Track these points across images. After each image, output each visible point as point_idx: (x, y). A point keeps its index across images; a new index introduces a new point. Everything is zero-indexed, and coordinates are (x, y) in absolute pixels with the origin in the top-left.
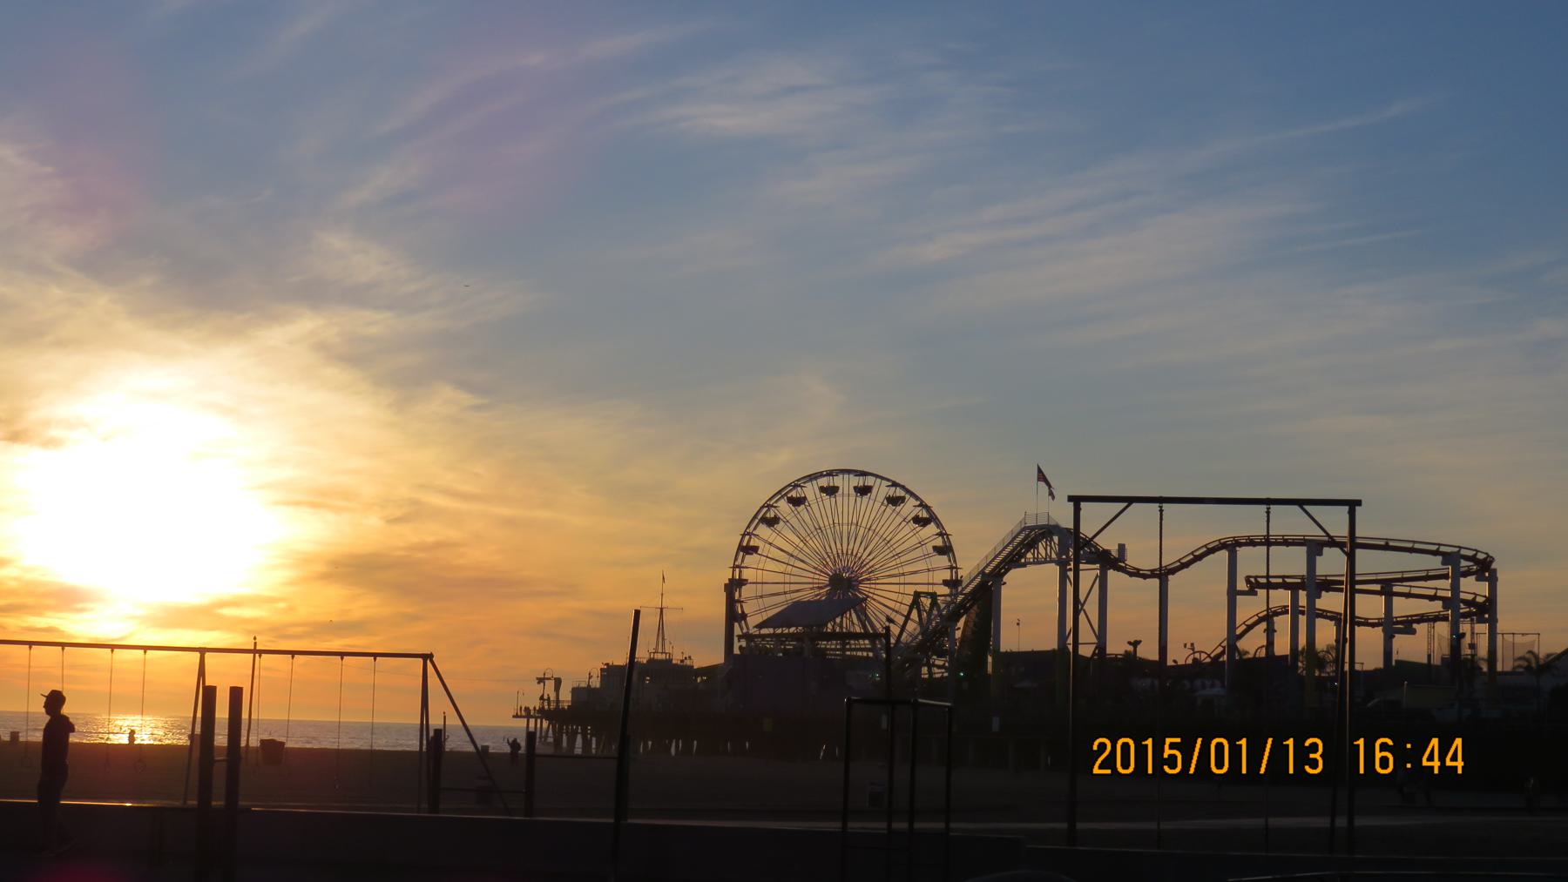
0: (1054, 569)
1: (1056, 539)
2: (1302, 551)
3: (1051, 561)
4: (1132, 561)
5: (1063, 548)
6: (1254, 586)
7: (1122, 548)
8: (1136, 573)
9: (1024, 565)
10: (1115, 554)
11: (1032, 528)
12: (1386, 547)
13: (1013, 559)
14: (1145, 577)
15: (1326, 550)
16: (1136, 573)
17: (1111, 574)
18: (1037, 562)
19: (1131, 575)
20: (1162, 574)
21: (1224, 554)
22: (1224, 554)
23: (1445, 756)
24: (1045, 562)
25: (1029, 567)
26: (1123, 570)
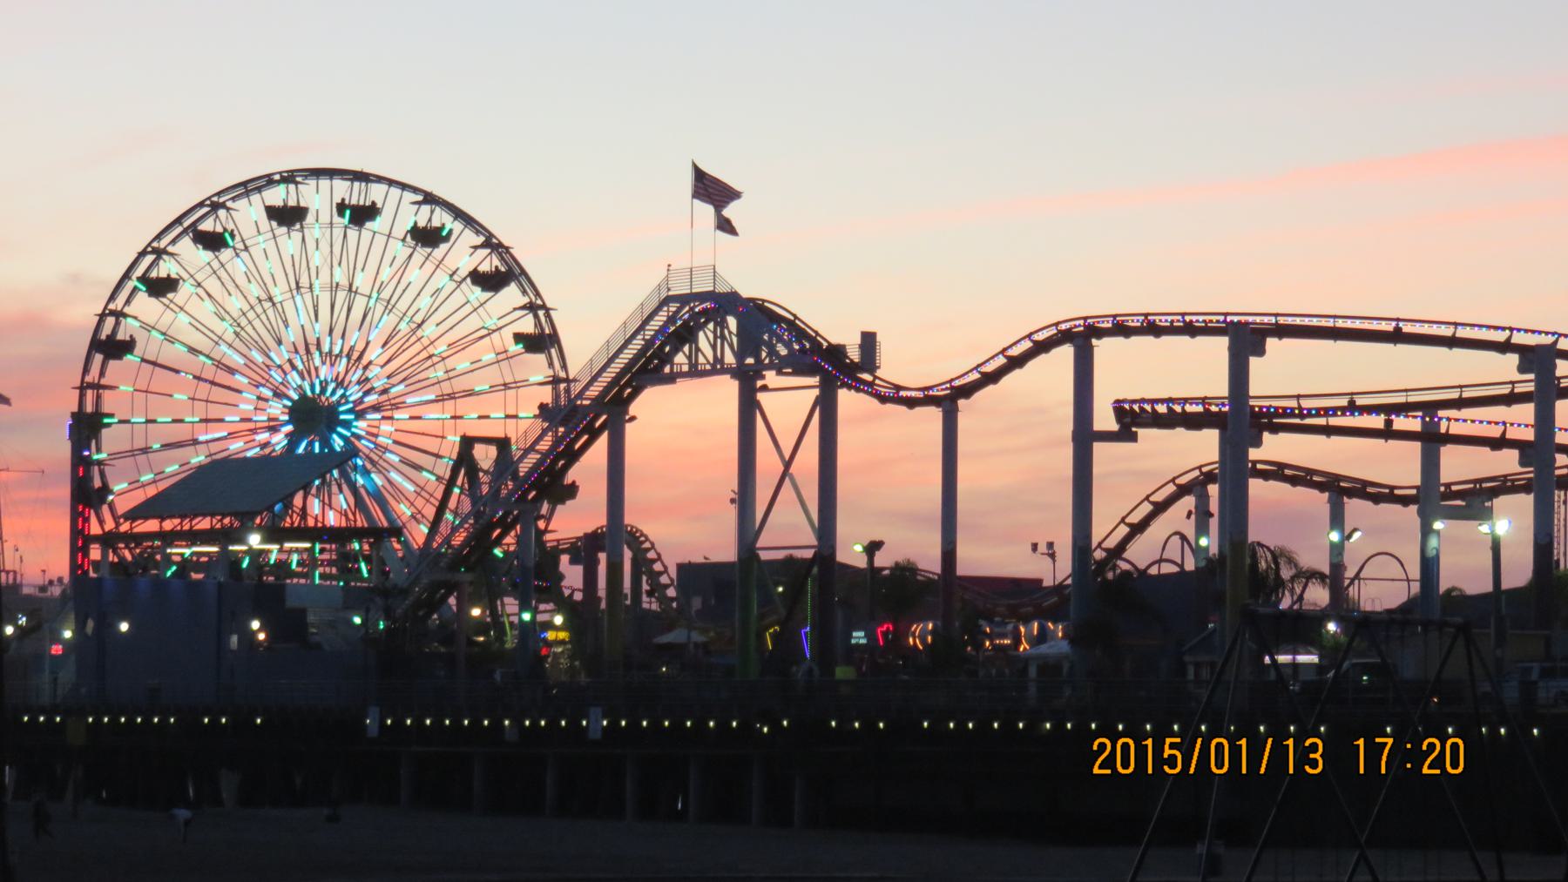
0: (728, 388)
1: (732, 322)
2: (1223, 342)
3: (723, 371)
4: (893, 368)
5: (748, 343)
6: (1132, 419)
7: (869, 341)
8: (895, 396)
9: (671, 379)
10: (854, 354)
11: (684, 299)
12: (1397, 337)
13: (650, 362)
14: (911, 403)
15: (1271, 342)
16: (895, 396)
17: (845, 397)
18: (695, 372)
19: (883, 399)
20: (949, 400)
21: (1066, 353)
22: (1066, 353)
23: (1446, 754)
24: (714, 371)
25: (682, 384)
26: (870, 389)
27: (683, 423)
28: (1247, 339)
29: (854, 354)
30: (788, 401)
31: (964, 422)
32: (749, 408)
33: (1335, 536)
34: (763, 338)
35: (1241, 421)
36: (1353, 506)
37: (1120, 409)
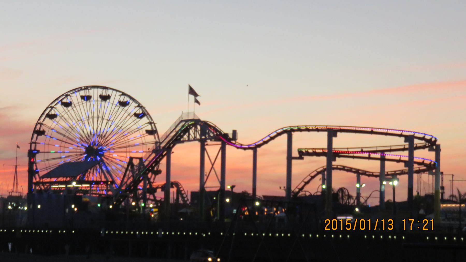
1: (199, 127)
4: (240, 140)
5: (203, 133)
6: (302, 154)
7: (235, 132)
9: (183, 142)
10: (231, 136)
11: (187, 121)
12: (372, 132)
14: (245, 149)
15: (339, 134)
16: (241, 147)
17: (228, 147)
18: (189, 140)
19: (238, 148)
20: (255, 148)
21: (285, 136)
22: (285, 136)
26: (234, 145)
28: (332, 133)
29: (231, 136)
30: (213, 149)
32: (203, 150)
34: (207, 132)
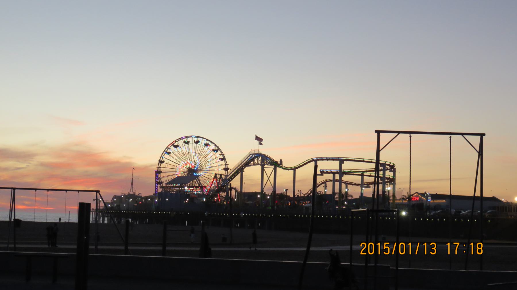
0: (260, 167)
1: (261, 158)
3: (259, 164)
4: (284, 164)
5: (263, 160)
7: (281, 161)
8: (286, 168)
9: (250, 166)
10: (279, 162)
11: (253, 154)
13: (247, 164)
14: (288, 170)
16: (286, 168)
17: (278, 168)
18: (254, 165)
19: (284, 169)
20: (294, 169)
24: (257, 165)
25: (252, 166)
26: (282, 167)
27: (253, 173)
28: (342, 161)
29: (279, 162)
30: (269, 169)
31: (296, 172)
32: (263, 170)
33: (346, 190)
34: (265, 160)
35: (342, 173)
36: (349, 186)
37: (320, 171)
